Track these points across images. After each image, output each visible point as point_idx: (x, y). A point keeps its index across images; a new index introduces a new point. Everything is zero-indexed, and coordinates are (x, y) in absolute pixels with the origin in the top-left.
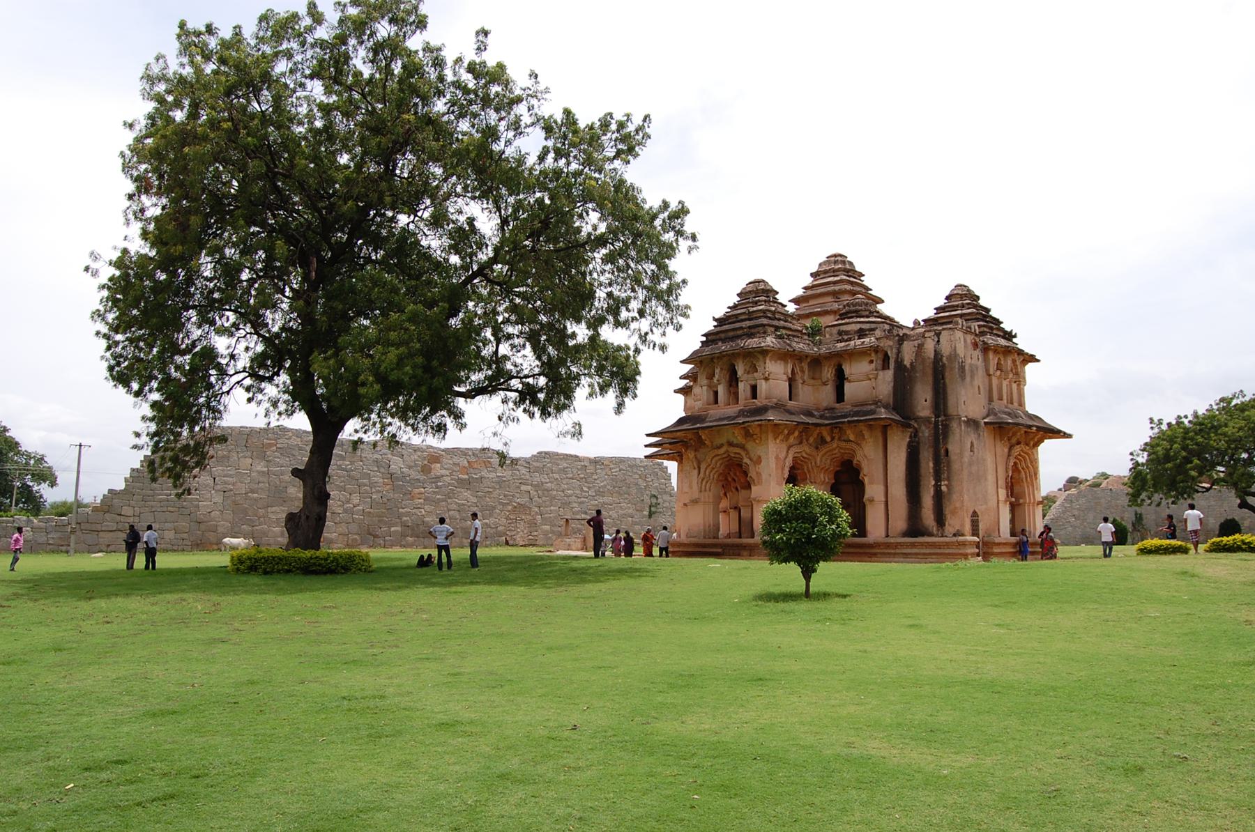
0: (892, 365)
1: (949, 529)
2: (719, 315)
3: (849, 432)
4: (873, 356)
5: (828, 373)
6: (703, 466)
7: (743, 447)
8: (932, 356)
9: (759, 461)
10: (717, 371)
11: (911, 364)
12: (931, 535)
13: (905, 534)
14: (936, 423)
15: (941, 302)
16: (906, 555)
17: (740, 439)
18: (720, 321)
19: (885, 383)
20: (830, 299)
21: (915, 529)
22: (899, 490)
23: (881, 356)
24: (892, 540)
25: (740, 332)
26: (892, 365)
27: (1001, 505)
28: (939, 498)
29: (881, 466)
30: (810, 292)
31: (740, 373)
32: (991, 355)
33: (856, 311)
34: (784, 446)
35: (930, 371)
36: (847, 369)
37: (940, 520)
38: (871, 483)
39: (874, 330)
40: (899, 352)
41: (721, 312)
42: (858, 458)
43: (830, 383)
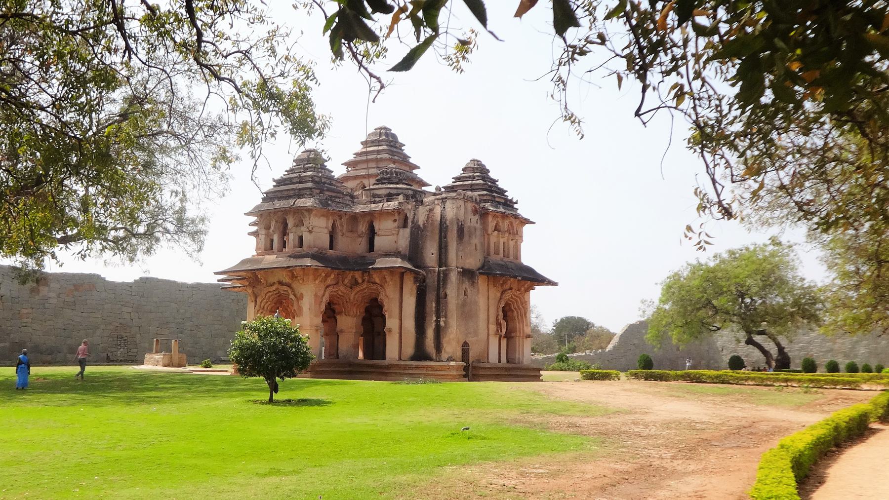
1: (444, 356)
2: (278, 177)
3: (375, 276)
4: (396, 216)
5: (363, 228)
7: (289, 286)
8: (439, 219)
9: (300, 298)
10: (273, 223)
11: (424, 224)
12: (431, 359)
13: (413, 358)
16: (411, 375)
17: (287, 280)
18: (280, 182)
19: (403, 240)
21: (420, 354)
22: (410, 324)
23: (402, 217)
24: (402, 363)
25: (292, 193)
29: (398, 304)
31: (290, 226)
34: (323, 286)
35: (437, 231)
36: (377, 227)
37: (438, 347)
38: (390, 317)
39: (399, 195)
40: (415, 214)
41: (280, 174)
42: (382, 297)
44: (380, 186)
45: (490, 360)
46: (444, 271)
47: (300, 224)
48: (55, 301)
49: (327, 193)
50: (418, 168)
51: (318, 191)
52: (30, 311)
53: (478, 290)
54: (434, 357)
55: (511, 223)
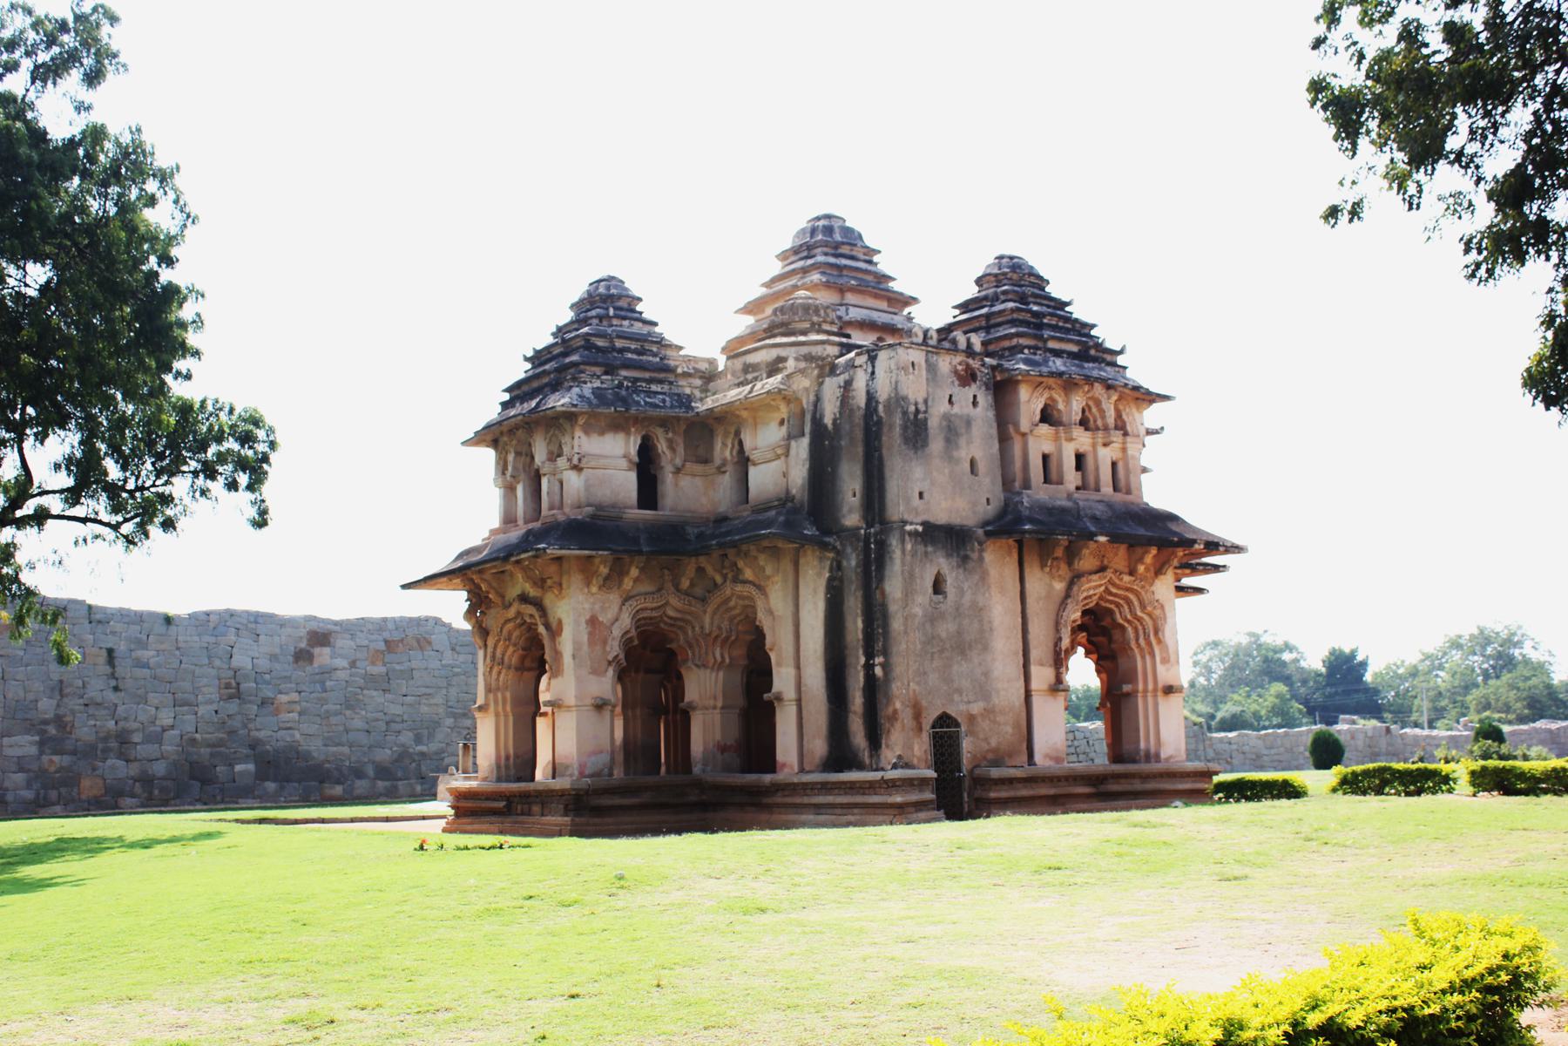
1: (889, 755)
6: (491, 641)
8: (863, 404)
11: (835, 420)
12: (861, 767)
14: (867, 536)
16: (818, 809)
21: (840, 756)
26: (807, 429)
27: (1037, 701)
28: (873, 688)
32: (1024, 392)
34: (614, 598)
35: (859, 434)
36: (748, 445)
37: (875, 738)
38: (779, 664)
43: (729, 468)
46: (876, 534)
48: (341, 675)
49: (624, 373)
51: (598, 370)
52: (295, 696)
53: (984, 577)
54: (867, 761)
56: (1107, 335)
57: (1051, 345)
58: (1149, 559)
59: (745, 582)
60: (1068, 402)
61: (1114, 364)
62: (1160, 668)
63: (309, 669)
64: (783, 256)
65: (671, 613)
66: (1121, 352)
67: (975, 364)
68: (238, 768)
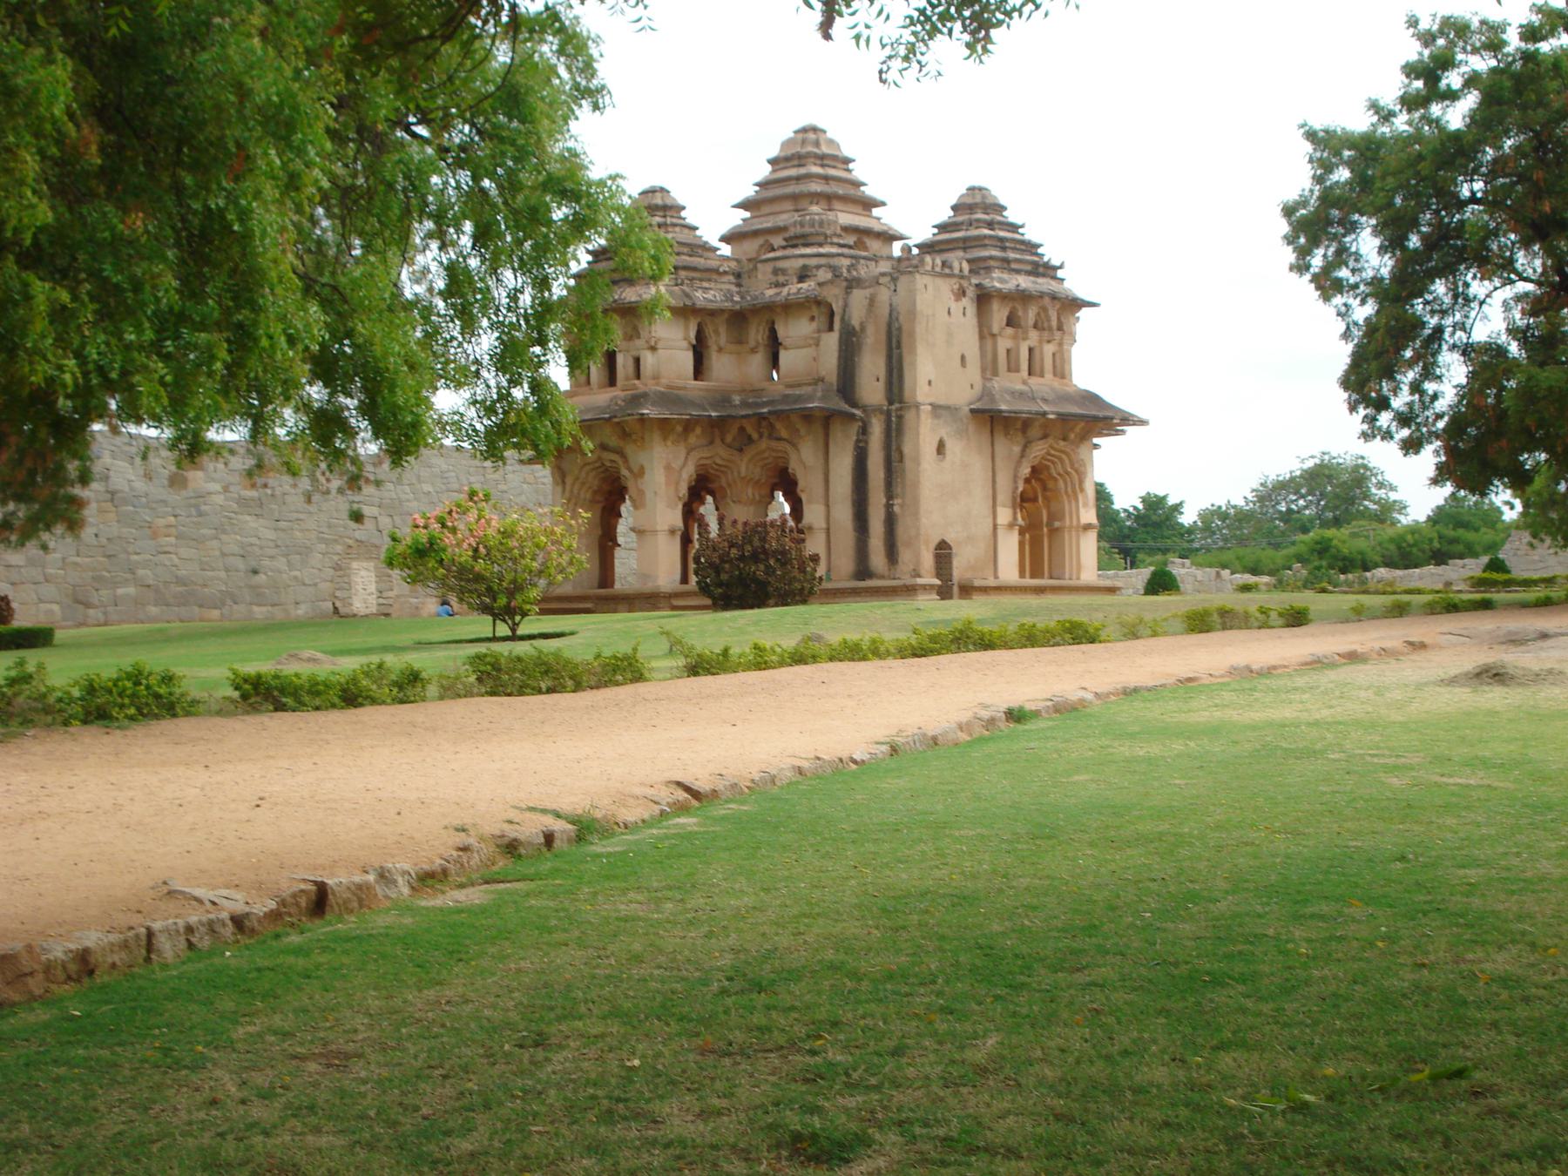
0: (837, 325)
3: (778, 426)
5: (757, 334)
6: (569, 480)
8: (886, 311)
9: (641, 472)
12: (882, 577)
15: (945, 214)
20: (788, 206)
22: (843, 513)
27: (1000, 532)
28: (890, 521)
29: (821, 477)
30: (771, 193)
32: (995, 305)
33: (803, 236)
34: (682, 451)
36: (781, 333)
37: (892, 553)
43: (761, 349)
44: (789, 252)
45: (1000, 574)
47: (633, 334)
50: (883, 204)
55: (1044, 309)
56: (1050, 254)
57: (1013, 266)
58: (1078, 429)
59: (779, 439)
60: (1025, 311)
61: (1054, 278)
62: (1082, 510)
63: (184, 493)
64: (773, 162)
65: (719, 461)
66: (1061, 267)
67: (965, 283)
68: (120, 591)
